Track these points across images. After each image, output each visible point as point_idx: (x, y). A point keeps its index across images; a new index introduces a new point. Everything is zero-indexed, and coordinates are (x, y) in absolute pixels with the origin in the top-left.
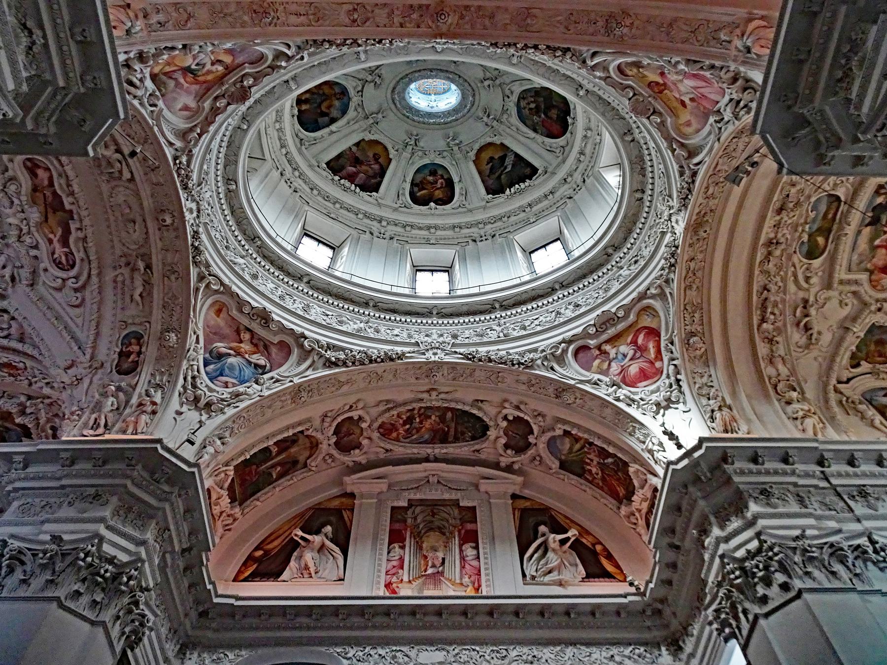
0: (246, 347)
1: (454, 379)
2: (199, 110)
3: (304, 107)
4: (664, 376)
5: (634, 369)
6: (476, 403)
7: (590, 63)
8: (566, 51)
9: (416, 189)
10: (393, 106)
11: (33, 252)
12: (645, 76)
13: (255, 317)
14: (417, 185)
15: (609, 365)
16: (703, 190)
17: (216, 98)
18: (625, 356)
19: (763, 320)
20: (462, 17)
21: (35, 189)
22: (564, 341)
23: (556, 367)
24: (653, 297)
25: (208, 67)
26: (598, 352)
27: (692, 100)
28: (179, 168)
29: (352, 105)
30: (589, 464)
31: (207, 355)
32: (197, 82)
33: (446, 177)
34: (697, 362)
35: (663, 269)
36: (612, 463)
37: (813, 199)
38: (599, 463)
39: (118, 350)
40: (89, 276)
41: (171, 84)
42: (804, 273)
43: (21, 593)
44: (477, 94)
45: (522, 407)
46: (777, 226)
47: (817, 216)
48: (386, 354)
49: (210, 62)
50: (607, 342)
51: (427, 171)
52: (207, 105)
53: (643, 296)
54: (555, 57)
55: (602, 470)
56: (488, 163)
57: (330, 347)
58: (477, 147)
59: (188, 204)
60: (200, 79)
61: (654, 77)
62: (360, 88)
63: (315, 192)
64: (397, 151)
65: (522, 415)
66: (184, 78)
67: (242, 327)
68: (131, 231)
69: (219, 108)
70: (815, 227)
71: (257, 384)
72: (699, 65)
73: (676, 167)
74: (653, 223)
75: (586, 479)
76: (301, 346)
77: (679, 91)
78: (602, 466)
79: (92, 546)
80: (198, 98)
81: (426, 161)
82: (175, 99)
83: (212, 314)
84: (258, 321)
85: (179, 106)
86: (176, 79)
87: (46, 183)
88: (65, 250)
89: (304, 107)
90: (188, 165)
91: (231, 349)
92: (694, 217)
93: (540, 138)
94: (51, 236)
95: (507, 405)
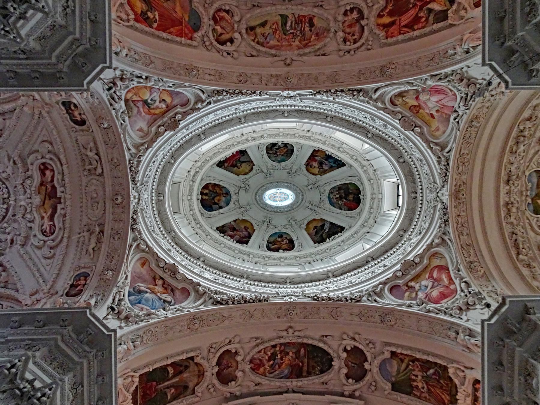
0: (159, 289)
1: (305, 317)
2: (147, 134)
3: (205, 197)
4: (459, 292)
5: (435, 293)
6: (322, 338)
7: (375, 97)
8: (359, 91)
9: (270, 245)
10: (255, 203)
11: (30, 225)
12: (407, 103)
13: (167, 271)
14: (271, 243)
15: (416, 294)
16: (455, 169)
17: (159, 126)
18: (426, 287)
19: (518, 254)
20: (300, 79)
21: (42, 184)
22: (381, 283)
23: (378, 299)
24: (438, 245)
25: (157, 103)
26: (406, 288)
27: (437, 111)
28: (131, 166)
29: (232, 201)
30: (414, 381)
31: (132, 290)
32: (150, 114)
33: (288, 238)
34: (480, 279)
35: (440, 227)
36: (434, 374)
37: (527, 173)
38: (422, 377)
39: (70, 283)
40: (62, 238)
41: (135, 110)
42: (536, 224)
44: (304, 195)
45: (357, 337)
46: (509, 193)
47: (533, 185)
48: (256, 297)
49: (159, 100)
50: (411, 280)
51: (277, 236)
52: (154, 129)
53: (430, 246)
54: (354, 95)
55: (427, 384)
56: (314, 229)
57: (216, 293)
58: (306, 222)
59: (133, 193)
60: (152, 111)
61: (412, 102)
62: (237, 191)
63: (209, 237)
64: (258, 225)
65: (357, 344)
66: (143, 108)
67: (157, 277)
68: (95, 208)
69: (160, 133)
70: (534, 194)
71: (164, 310)
72: (438, 77)
73: (435, 159)
74: (426, 208)
75: (415, 396)
76: (197, 291)
77: (429, 108)
78: (426, 379)
79: (19, 361)
80: (150, 123)
81: (276, 231)
82: (136, 122)
83: (139, 265)
84: (169, 273)
85: (137, 128)
86: (138, 107)
87: (49, 179)
88: (51, 223)
89: (205, 197)
90: (138, 166)
91: (149, 288)
92: (454, 188)
93: (344, 212)
94: (44, 215)
95: (345, 337)
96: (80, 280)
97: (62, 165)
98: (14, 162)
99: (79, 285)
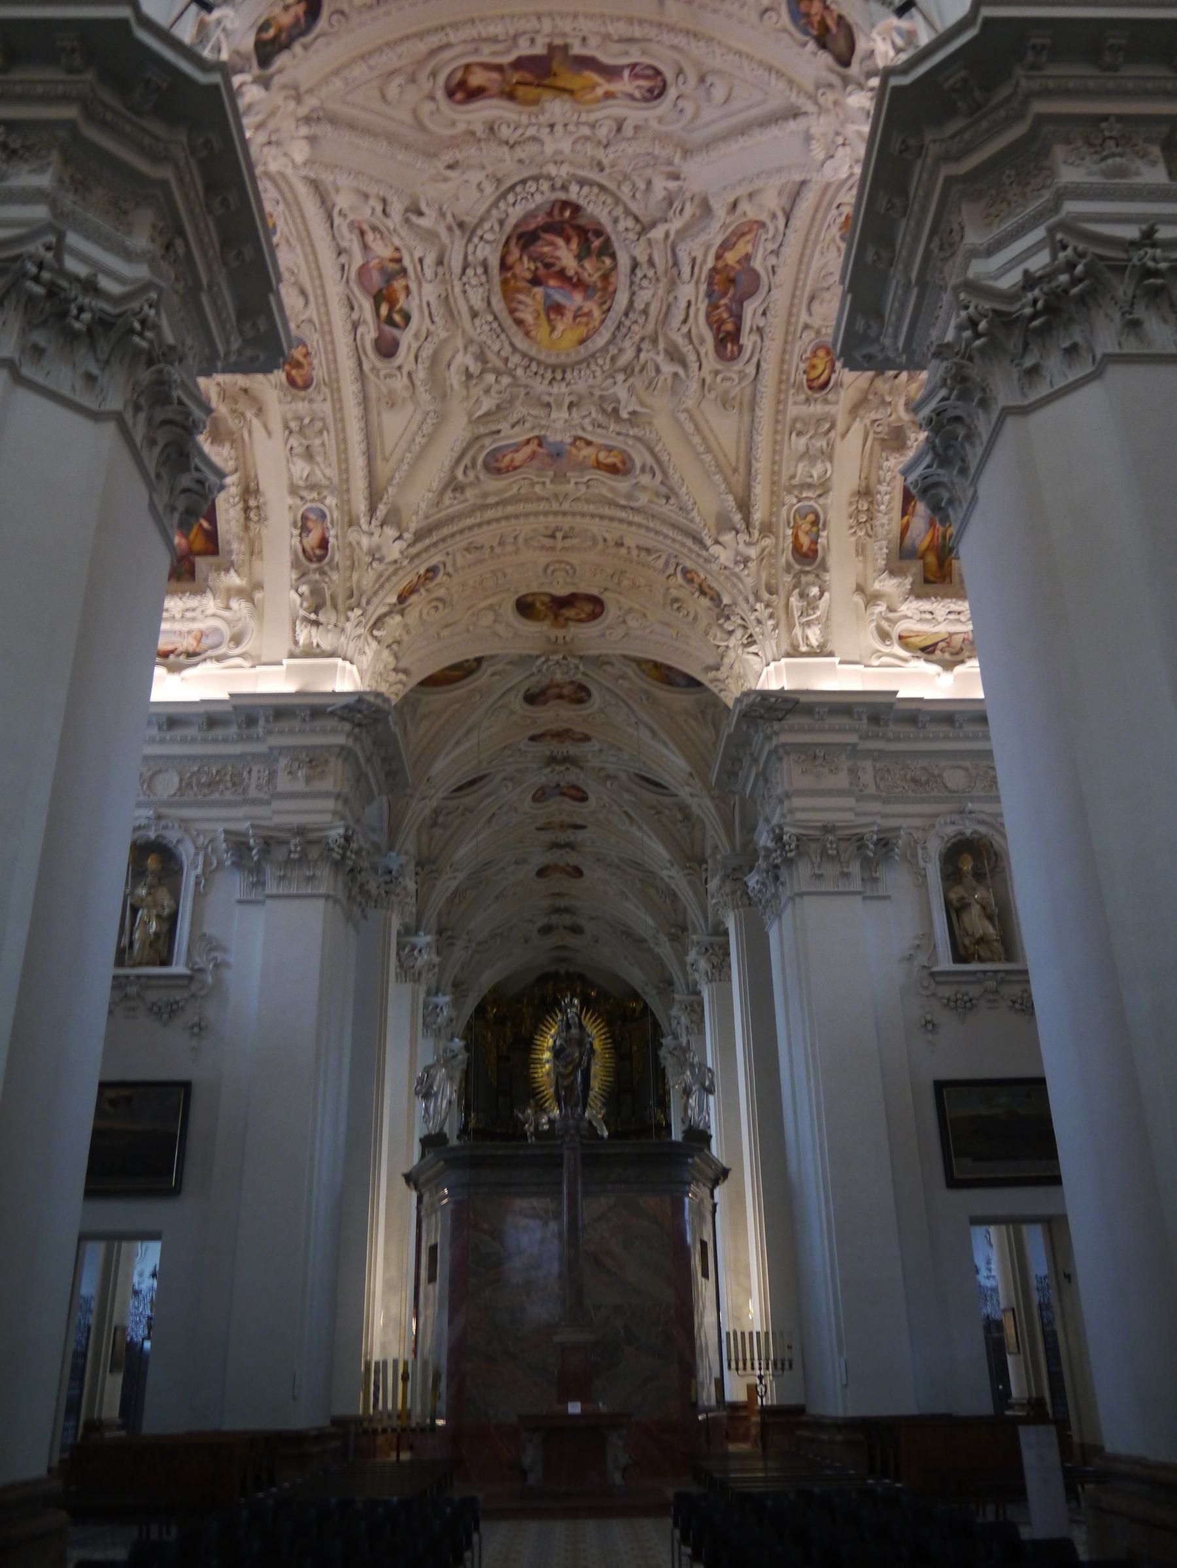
11: (628, 131)
21: (511, 96)
79: (966, 308)
87: (495, 75)
88: (626, 73)
94: (600, 91)
96: (807, 15)
97: (448, 46)
98: (450, 167)
99: (823, 22)
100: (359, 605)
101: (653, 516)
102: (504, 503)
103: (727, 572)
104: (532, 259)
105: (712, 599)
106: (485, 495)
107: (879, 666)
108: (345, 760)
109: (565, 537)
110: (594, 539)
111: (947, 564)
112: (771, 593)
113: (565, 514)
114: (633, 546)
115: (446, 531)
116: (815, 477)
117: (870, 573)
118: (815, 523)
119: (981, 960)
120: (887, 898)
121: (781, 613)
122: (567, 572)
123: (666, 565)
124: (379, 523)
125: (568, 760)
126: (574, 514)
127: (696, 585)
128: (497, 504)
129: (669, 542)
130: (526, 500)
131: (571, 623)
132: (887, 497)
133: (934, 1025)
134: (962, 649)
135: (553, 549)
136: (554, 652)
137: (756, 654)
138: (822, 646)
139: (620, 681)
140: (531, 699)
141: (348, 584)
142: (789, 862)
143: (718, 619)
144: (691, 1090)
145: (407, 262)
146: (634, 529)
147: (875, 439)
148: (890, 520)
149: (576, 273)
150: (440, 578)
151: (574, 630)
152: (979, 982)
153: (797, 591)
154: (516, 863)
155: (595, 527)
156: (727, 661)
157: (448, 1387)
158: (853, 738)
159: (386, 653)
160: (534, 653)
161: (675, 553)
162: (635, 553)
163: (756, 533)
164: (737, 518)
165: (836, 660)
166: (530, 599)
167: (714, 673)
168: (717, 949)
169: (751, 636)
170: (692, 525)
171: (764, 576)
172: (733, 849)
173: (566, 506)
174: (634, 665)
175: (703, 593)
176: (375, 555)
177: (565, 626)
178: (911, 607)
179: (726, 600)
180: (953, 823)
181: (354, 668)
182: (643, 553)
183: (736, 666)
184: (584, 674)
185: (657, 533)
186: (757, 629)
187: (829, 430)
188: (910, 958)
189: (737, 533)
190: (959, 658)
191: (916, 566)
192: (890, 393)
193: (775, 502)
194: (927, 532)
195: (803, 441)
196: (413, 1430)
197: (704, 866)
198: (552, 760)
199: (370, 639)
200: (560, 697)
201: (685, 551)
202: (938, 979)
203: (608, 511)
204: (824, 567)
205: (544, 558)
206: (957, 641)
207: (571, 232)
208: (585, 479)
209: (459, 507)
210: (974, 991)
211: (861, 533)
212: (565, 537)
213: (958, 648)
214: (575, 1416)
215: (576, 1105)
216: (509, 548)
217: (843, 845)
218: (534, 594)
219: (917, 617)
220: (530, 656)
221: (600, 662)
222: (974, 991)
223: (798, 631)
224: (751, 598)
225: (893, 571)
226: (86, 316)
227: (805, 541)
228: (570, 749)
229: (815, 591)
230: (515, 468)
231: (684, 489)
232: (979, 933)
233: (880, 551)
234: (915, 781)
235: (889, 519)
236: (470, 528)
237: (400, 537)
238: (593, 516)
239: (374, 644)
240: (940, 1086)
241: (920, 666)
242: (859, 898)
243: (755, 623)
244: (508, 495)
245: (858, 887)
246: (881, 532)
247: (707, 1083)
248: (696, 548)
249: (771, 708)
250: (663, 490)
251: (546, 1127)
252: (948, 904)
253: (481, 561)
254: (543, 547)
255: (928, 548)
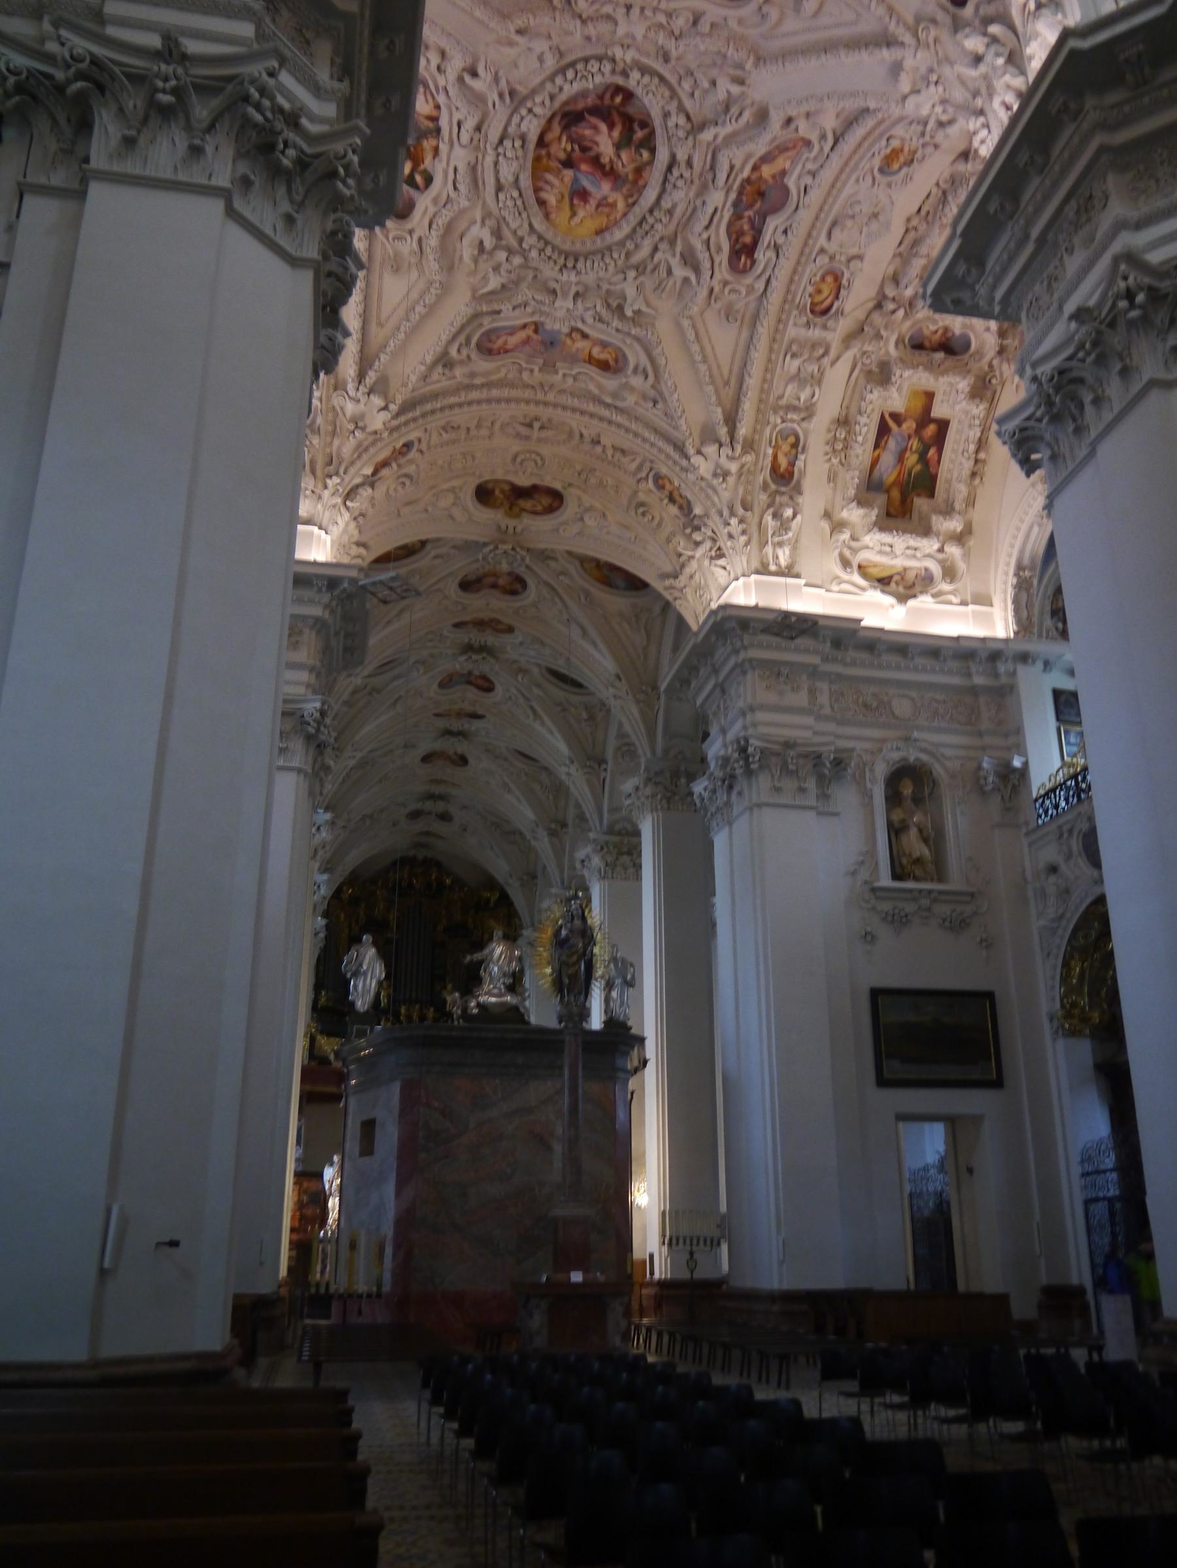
11: (704, 27)
43: (1108, 416)
79: (1125, 278)
98: (519, 32)
100: (337, 474)
101: (637, 419)
102: (489, 385)
103: (703, 484)
104: (571, 140)
105: (681, 508)
106: (473, 375)
107: (839, 592)
108: (318, 632)
109: (542, 428)
110: (571, 434)
111: (909, 500)
112: (746, 509)
113: (546, 404)
114: (609, 445)
115: (429, 407)
116: (802, 400)
117: (839, 500)
118: (795, 445)
119: (916, 879)
120: (836, 814)
121: (754, 529)
122: (536, 463)
123: (640, 468)
124: (366, 390)
125: (483, 649)
126: (555, 406)
127: (666, 493)
128: (483, 385)
129: (647, 446)
130: (512, 385)
131: (524, 514)
132: (865, 430)
133: (873, 937)
134: (914, 584)
135: (527, 438)
136: (504, 542)
137: (725, 568)
138: (790, 567)
139: (561, 578)
140: (466, 585)
141: (328, 450)
142: (749, 773)
143: (685, 528)
144: (614, 983)
145: (444, 123)
146: (613, 428)
147: (861, 370)
148: (864, 451)
149: (611, 161)
150: (413, 454)
151: (527, 521)
152: (915, 899)
153: (771, 511)
154: (405, 746)
155: (574, 422)
156: (688, 571)
157: (394, 1255)
158: (815, 660)
159: (353, 525)
160: (482, 540)
161: (652, 458)
162: (610, 452)
163: (739, 448)
164: (723, 432)
165: (802, 582)
166: (490, 486)
167: (671, 581)
168: (611, 848)
169: (719, 549)
170: (676, 434)
171: (741, 491)
172: (654, 753)
173: (551, 397)
174: (577, 563)
175: (672, 500)
176: (357, 422)
177: (518, 516)
178: (874, 539)
179: (698, 511)
180: (898, 749)
181: (328, 538)
182: (618, 455)
183: (697, 577)
184: (527, 567)
185: (636, 435)
186: (729, 543)
187: (823, 356)
188: (854, 873)
189: (721, 445)
190: (911, 592)
191: (881, 499)
192: (886, 327)
193: (761, 419)
194: (895, 467)
195: (796, 363)
196: (360, 1296)
197: (604, 766)
198: (469, 648)
199: (343, 509)
200: (494, 586)
201: (662, 457)
202: (878, 894)
203: (591, 408)
204: (798, 490)
205: (516, 447)
206: (911, 576)
207: (616, 118)
208: (574, 372)
209: (445, 383)
210: (910, 908)
211: (835, 461)
212: (542, 428)
213: (910, 583)
214: (577, 1285)
215: (580, 993)
216: (484, 432)
217: (801, 761)
218: (496, 481)
219: (877, 548)
220: (476, 543)
221: (544, 556)
222: (910, 908)
223: (769, 549)
224: (726, 513)
225: (861, 502)
226: (291, 152)
227: (783, 462)
228: (490, 639)
229: (789, 512)
230: (506, 351)
231: (676, 396)
232: (916, 854)
233: (852, 480)
234: (866, 706)
235: (862, 451)
236: (451, 407)
237: (385, 408)
238: (574, 410)
239: (347, 516)
240: (876, 994)
241: (877, 596)
242: (811, 814)
243: (726, 537)
244: (494, 377)
245: (812, 802)
246: (855, 462)
247: (629, 977)
248: (676, 456)
249: (790, 627)
250: (652, 393)
251: (475, 1011)
252: (890, 825)
253: (454, 442)
254: (518, 435)
255: (894, 483)
